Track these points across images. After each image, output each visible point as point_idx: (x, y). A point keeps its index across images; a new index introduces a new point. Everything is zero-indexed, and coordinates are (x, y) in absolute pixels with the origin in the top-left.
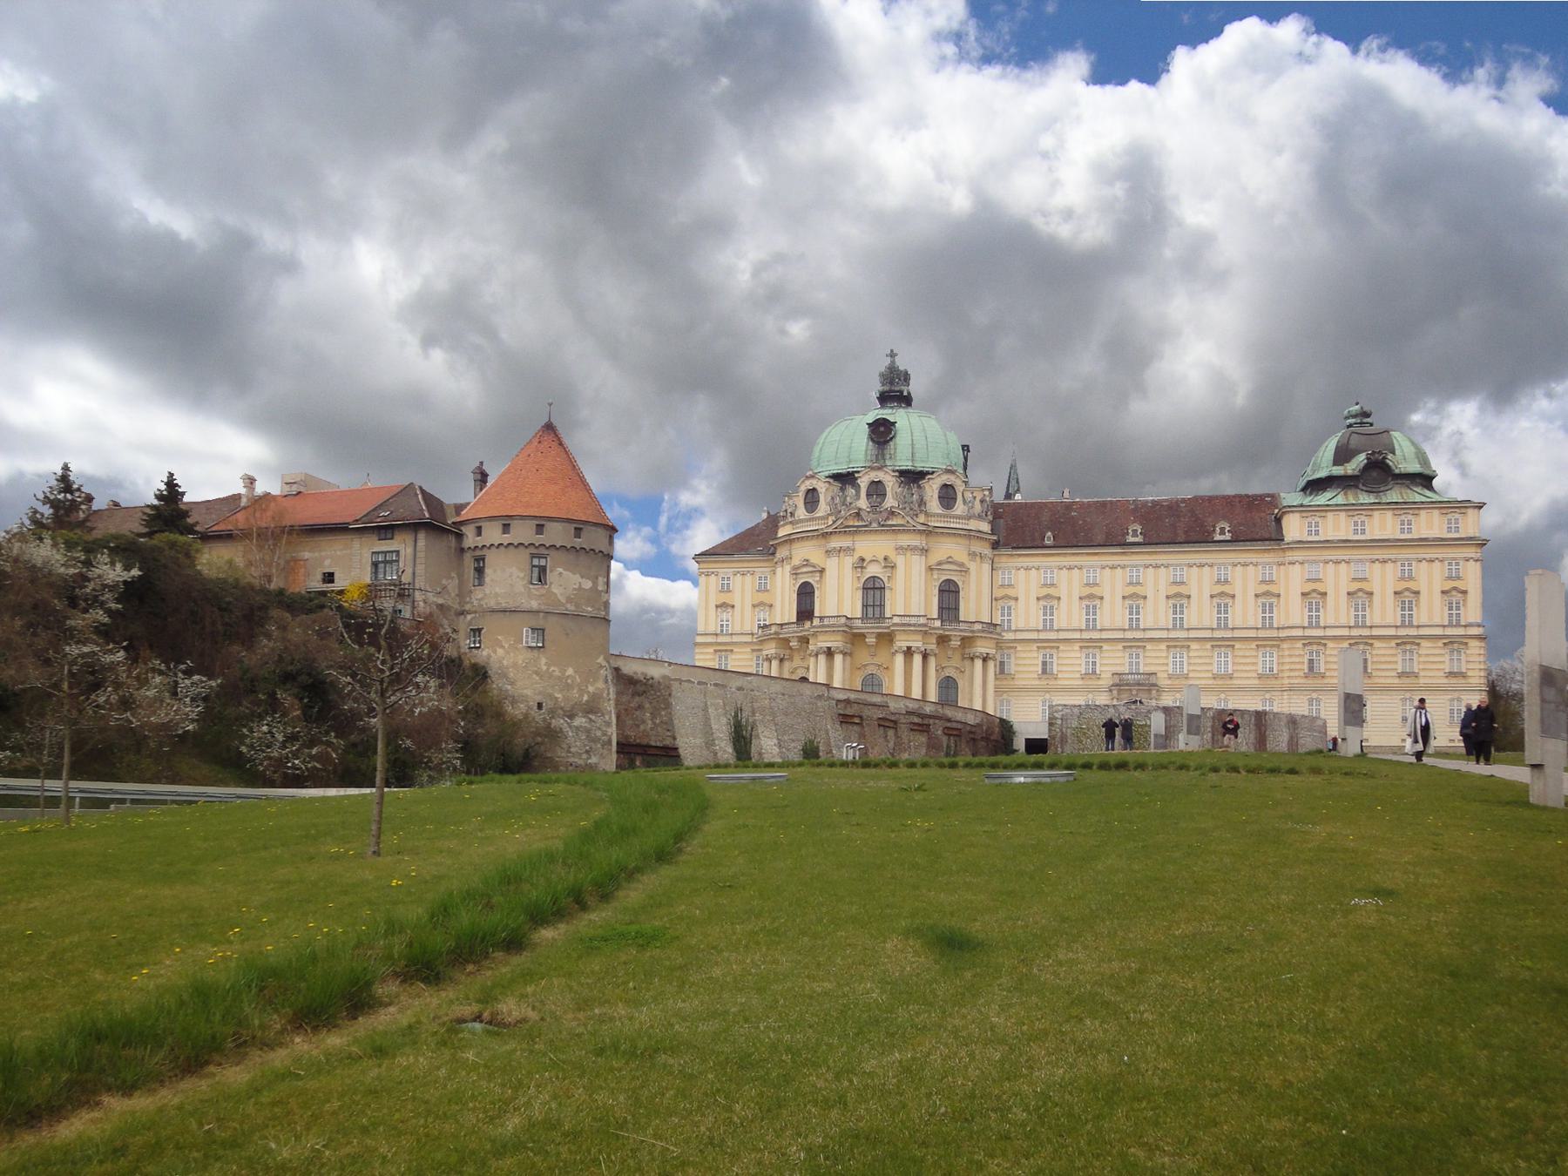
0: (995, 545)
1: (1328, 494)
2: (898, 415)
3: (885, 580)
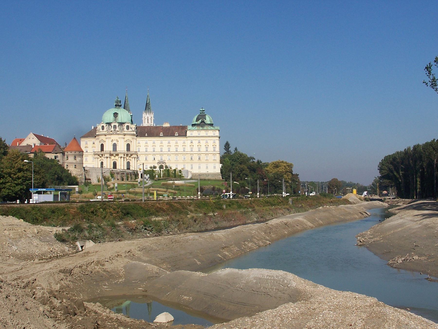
1: (195, 127)
3: (117, 144)
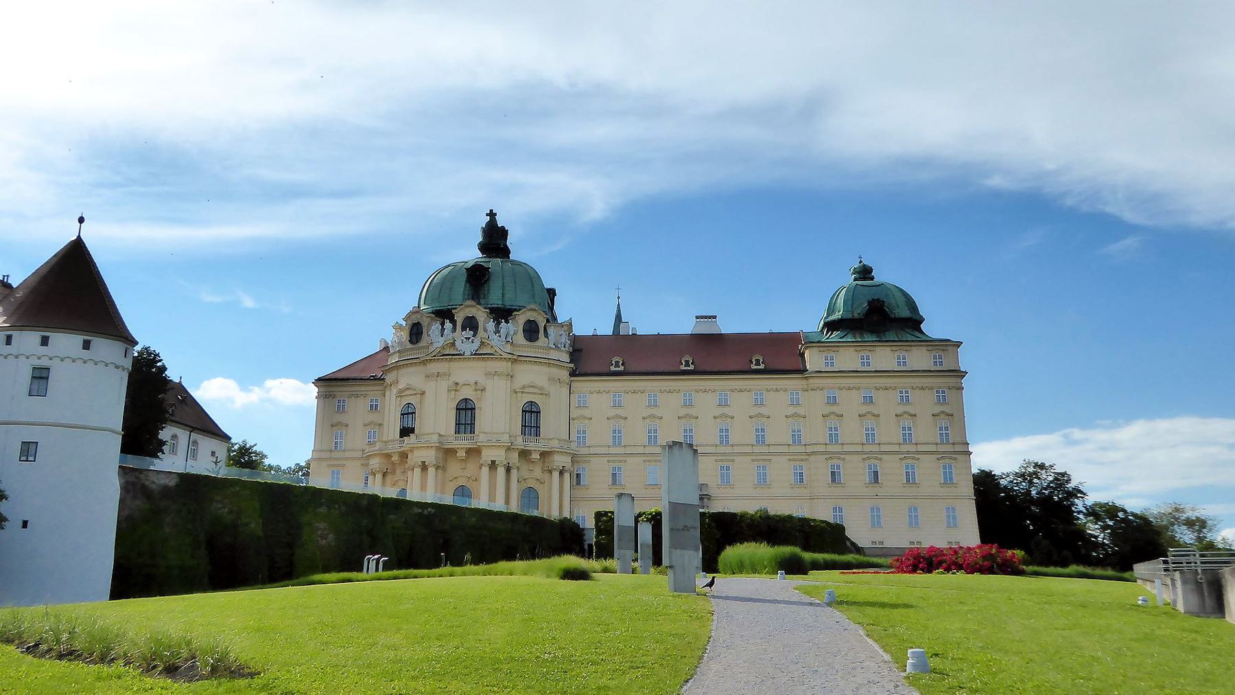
0: (573, 374)
2: (495, 264)
